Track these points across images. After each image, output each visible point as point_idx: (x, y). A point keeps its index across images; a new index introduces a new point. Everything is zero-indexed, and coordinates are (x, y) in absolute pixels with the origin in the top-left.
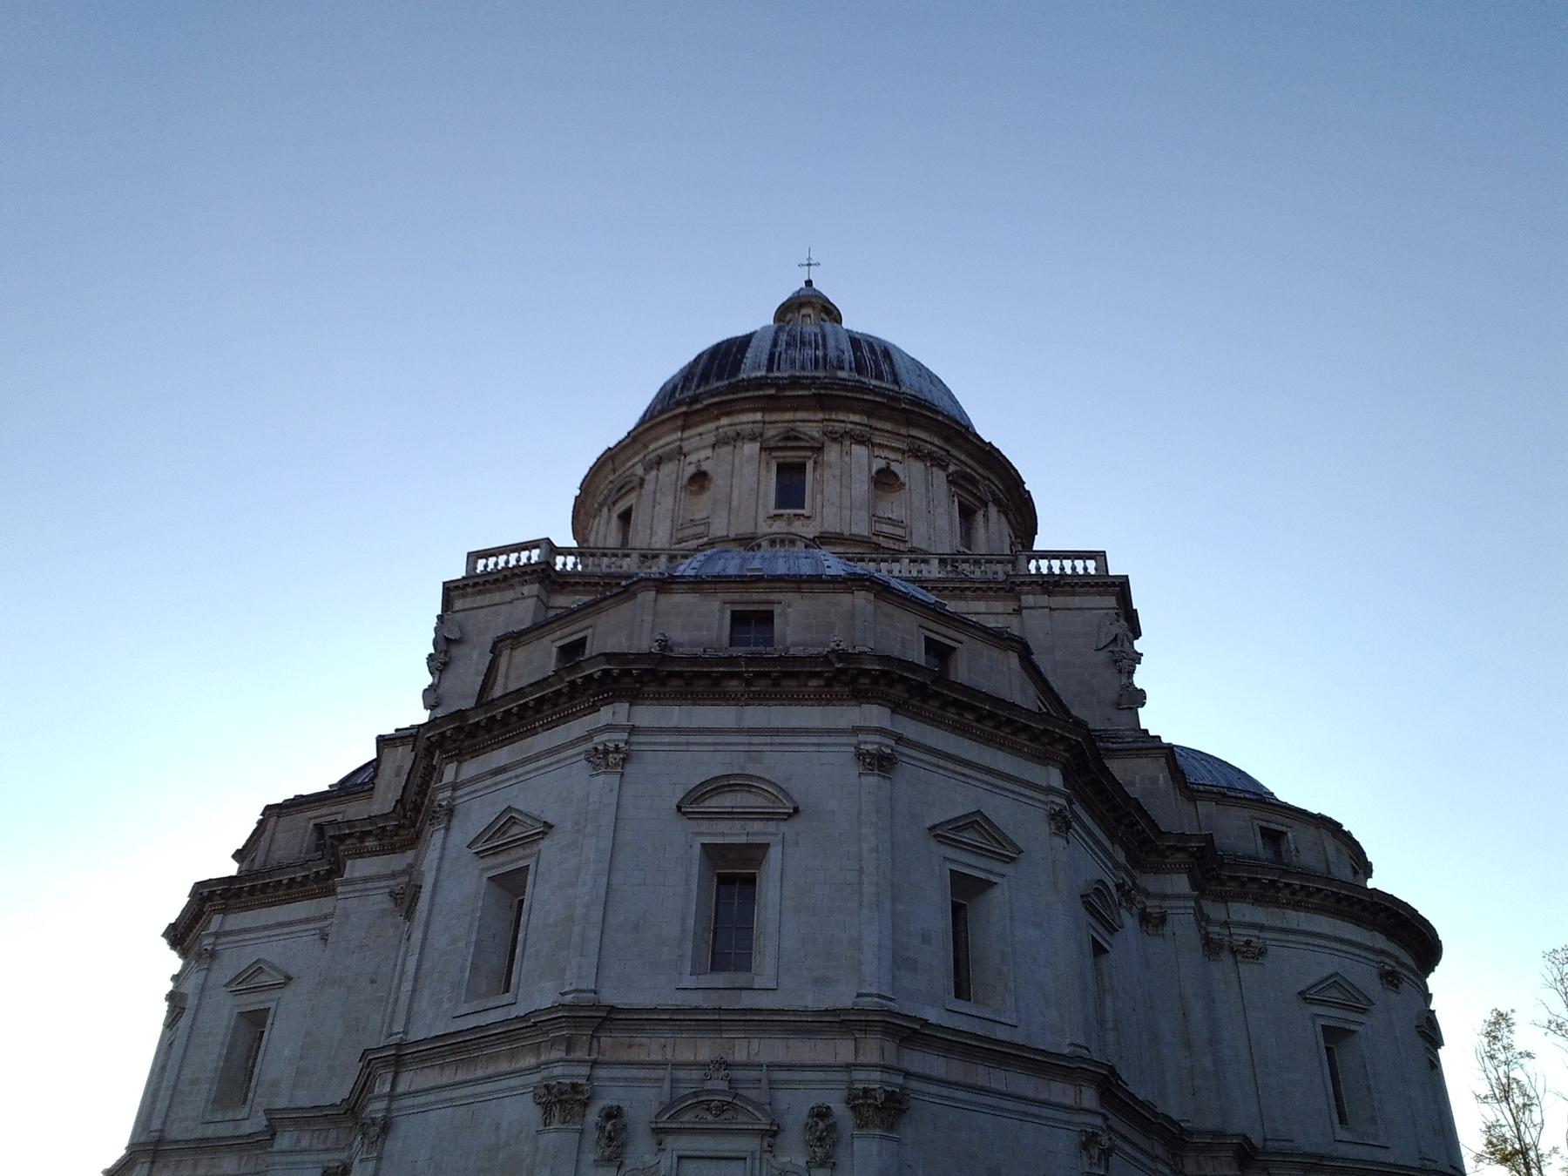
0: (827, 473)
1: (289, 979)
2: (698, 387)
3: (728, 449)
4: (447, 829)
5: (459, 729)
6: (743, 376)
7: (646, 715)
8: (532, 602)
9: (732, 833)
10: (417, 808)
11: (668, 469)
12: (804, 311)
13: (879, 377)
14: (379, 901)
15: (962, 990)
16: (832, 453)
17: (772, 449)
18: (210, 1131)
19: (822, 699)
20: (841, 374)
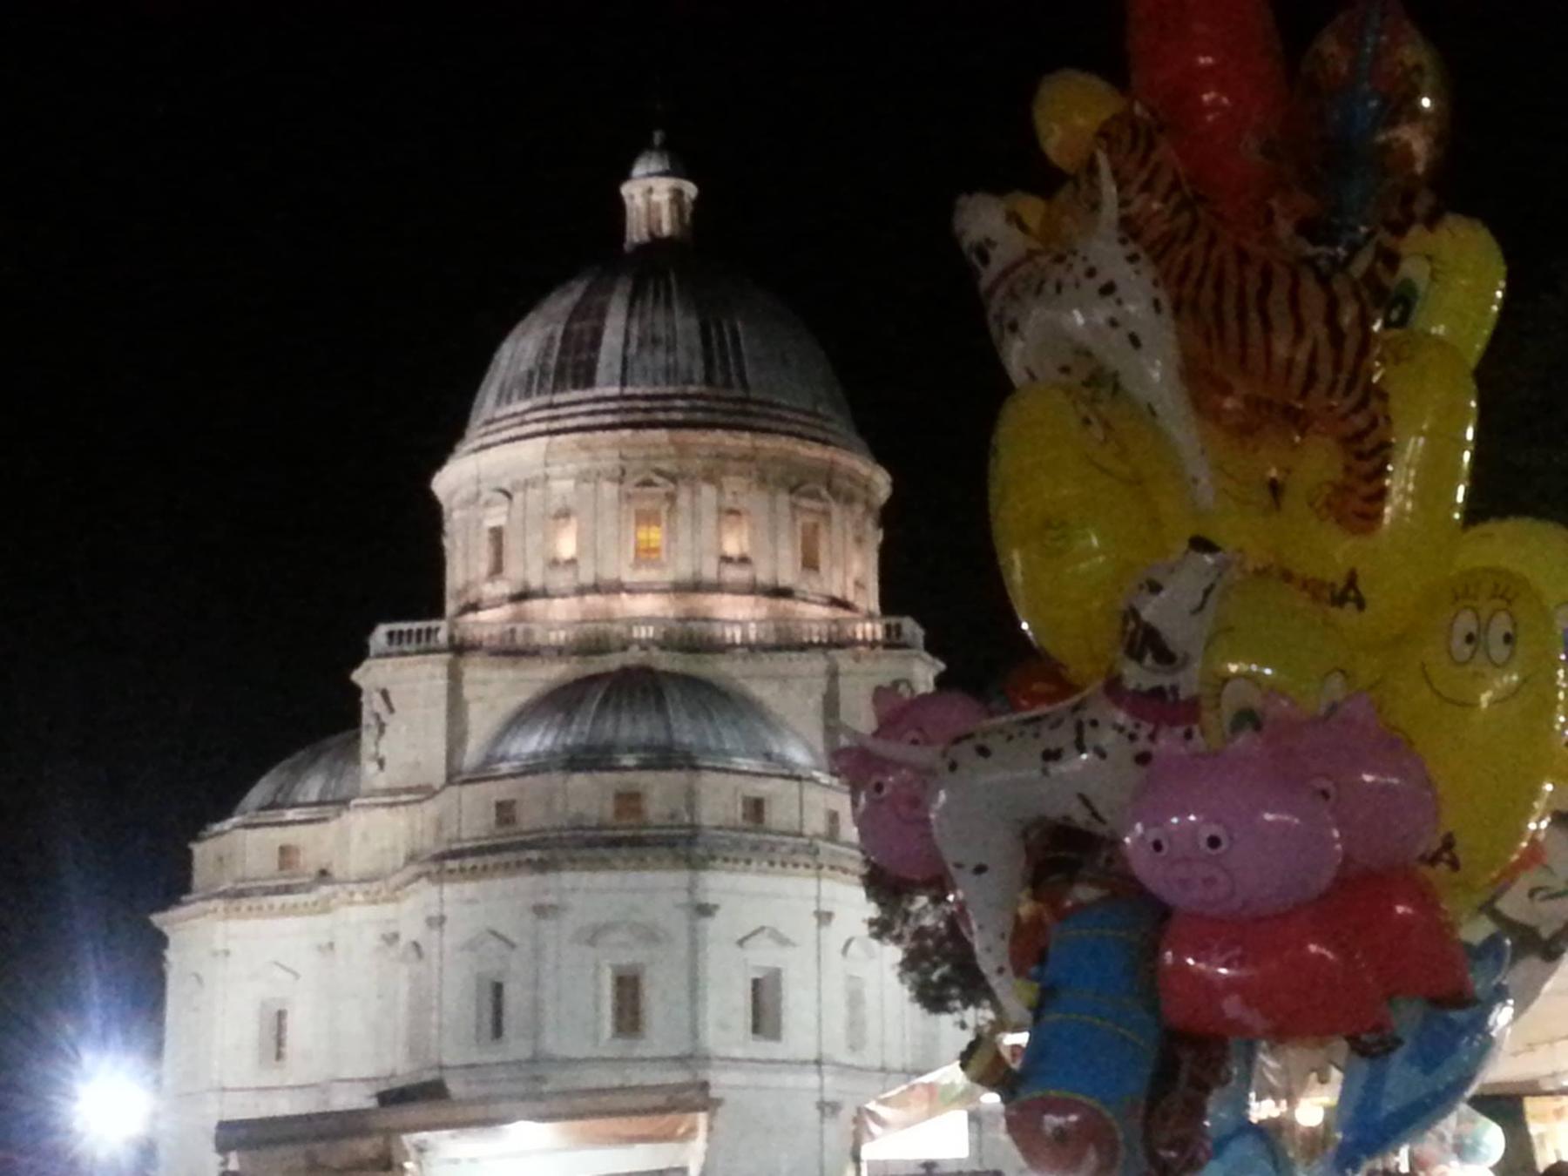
0: (680, 520)
1: (296, 975)
2: (555, 390)
3: (587, 488)
4: (442, 931)
5: (439, 873)
6: (598, 391)
7: (568, 878)
8: (442, 683)
9: (625, 958)
10: (398, 888)
11: (534, 494)
12: (655, 197)
13: (728, 384)
14: (371, 937)
15: (756, 1028)
16: (684, 499)
17: (629, 496)
18: (263, 1084)
19: (675, 866)
20: (692, 389)
